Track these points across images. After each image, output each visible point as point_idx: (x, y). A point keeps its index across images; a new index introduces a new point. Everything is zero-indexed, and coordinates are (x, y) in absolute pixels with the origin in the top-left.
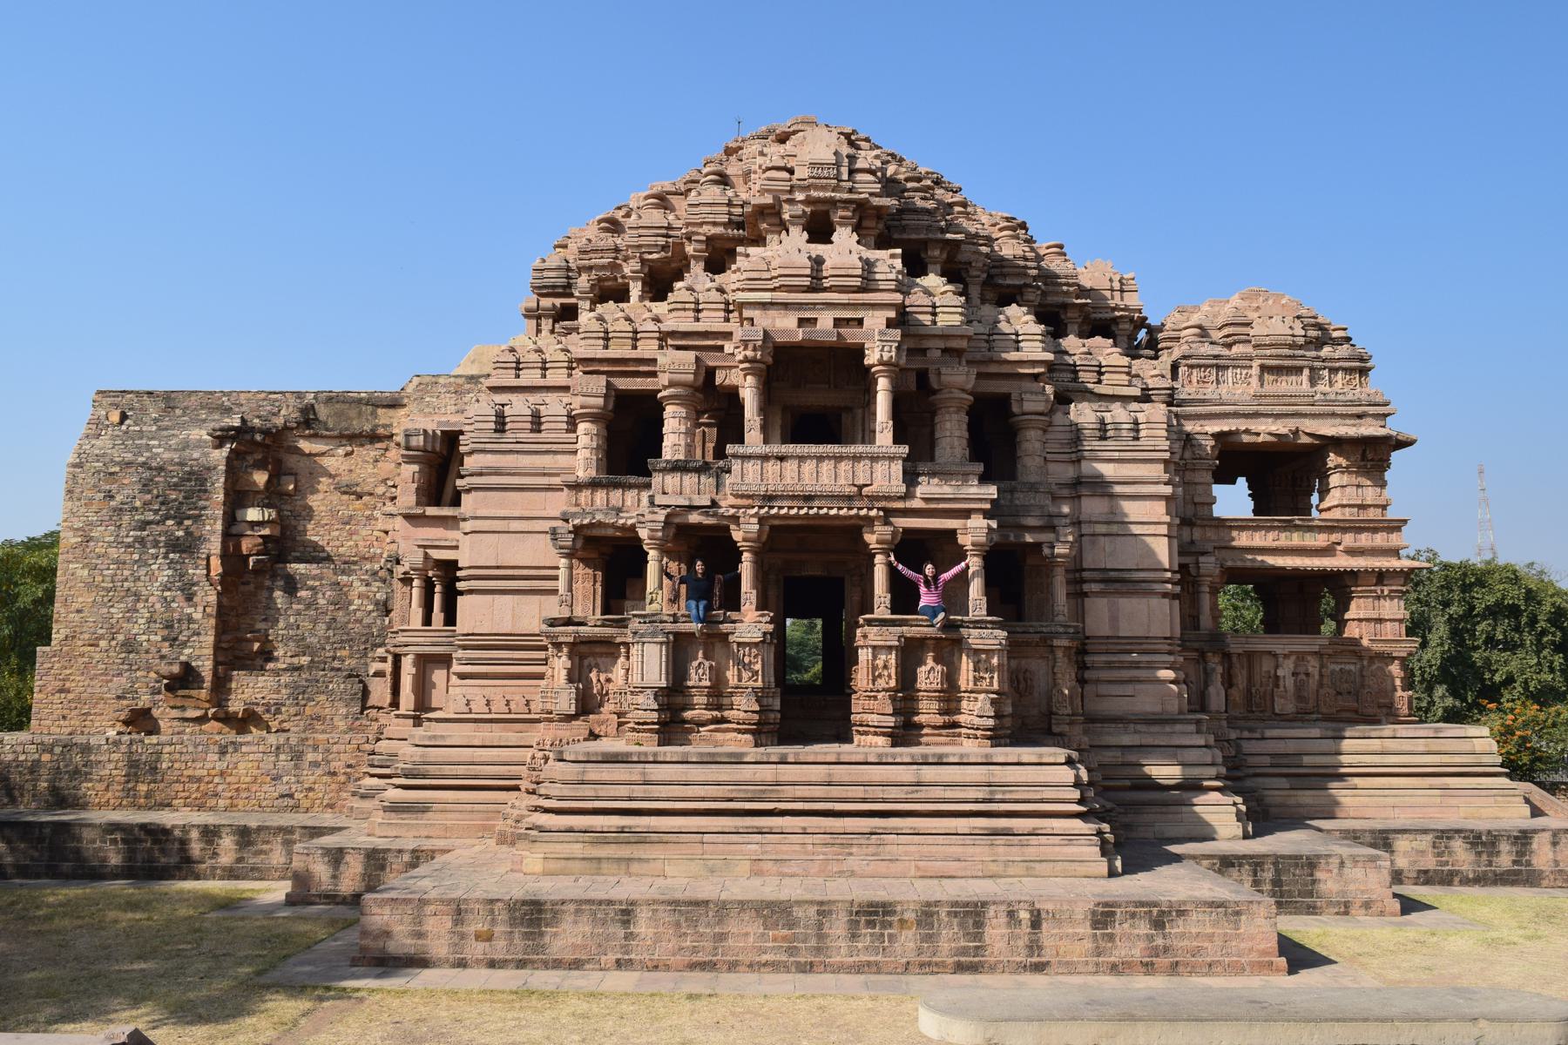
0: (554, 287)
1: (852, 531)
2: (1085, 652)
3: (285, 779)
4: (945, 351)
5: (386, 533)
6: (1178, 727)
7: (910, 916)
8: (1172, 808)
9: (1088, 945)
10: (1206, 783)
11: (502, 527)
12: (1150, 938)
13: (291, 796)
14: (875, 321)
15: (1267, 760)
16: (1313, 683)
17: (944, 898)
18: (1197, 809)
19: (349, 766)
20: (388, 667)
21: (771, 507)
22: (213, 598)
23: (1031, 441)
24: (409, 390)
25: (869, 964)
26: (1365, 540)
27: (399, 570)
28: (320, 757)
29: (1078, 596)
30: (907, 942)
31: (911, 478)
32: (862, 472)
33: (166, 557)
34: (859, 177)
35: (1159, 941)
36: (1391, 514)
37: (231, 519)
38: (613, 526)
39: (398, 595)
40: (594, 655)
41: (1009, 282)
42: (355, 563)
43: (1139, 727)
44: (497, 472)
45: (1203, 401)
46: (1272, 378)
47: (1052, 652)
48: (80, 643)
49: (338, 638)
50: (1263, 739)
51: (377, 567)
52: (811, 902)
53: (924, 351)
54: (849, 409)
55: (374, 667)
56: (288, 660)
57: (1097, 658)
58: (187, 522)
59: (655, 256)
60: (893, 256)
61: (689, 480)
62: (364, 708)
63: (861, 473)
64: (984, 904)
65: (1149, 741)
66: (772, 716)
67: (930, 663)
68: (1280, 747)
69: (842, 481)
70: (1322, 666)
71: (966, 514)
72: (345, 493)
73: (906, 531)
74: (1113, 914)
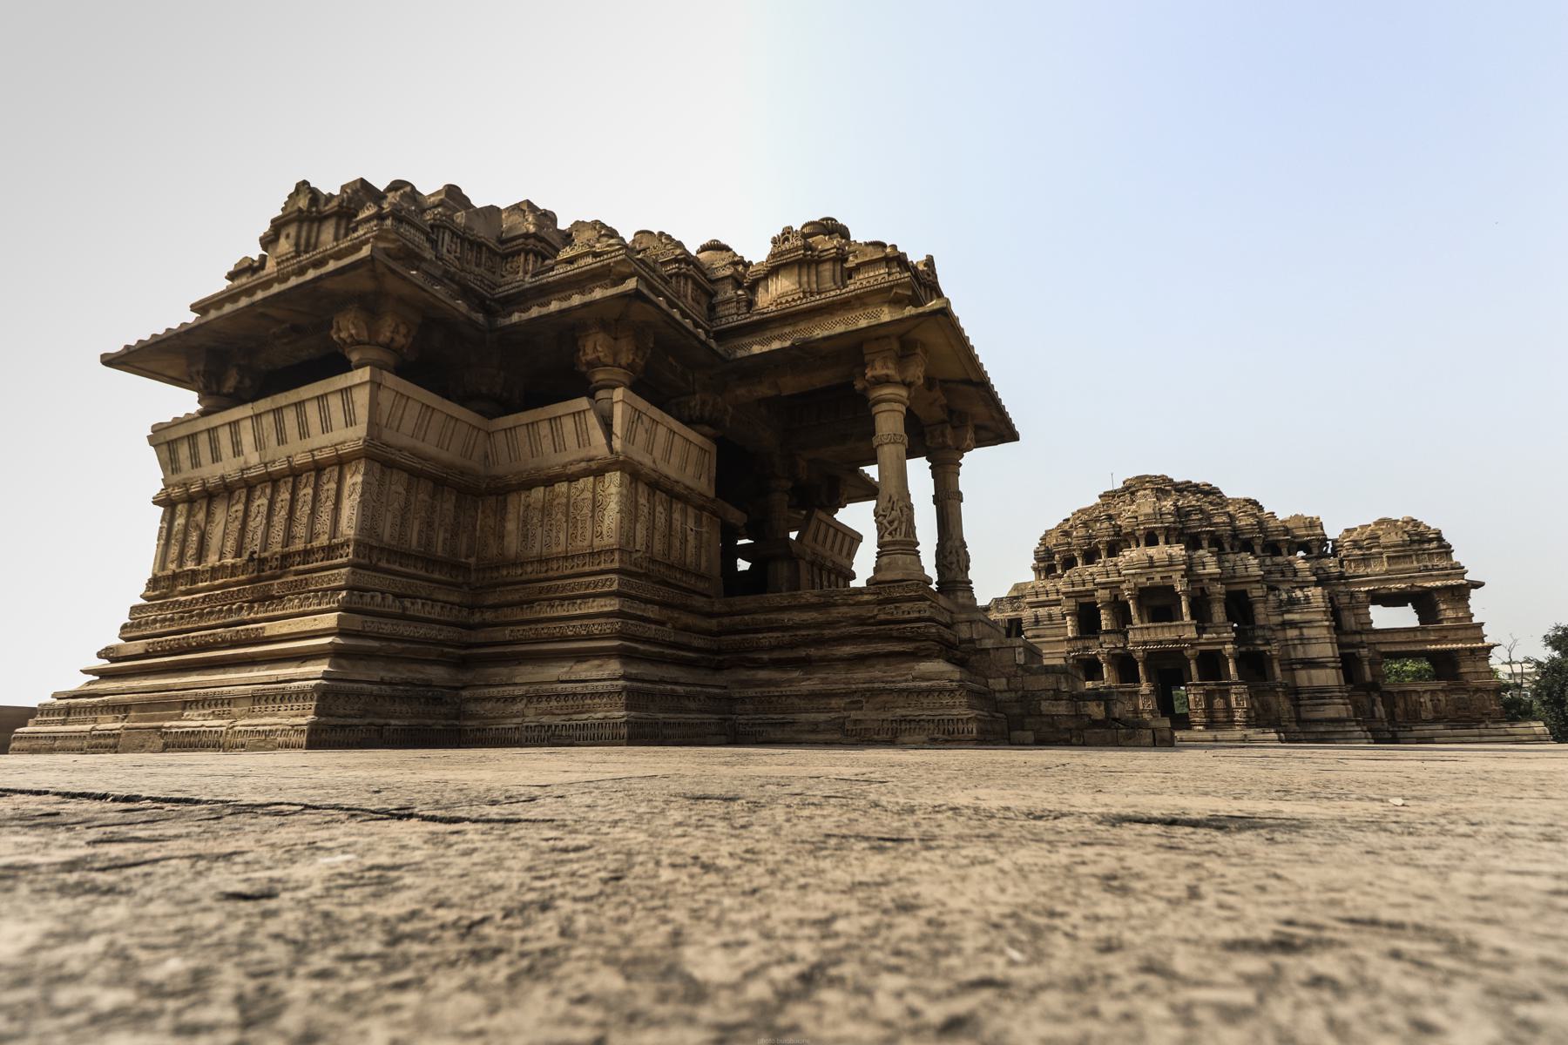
14: (1177, 576)
16: (1443, 704)
71: (1225, 643)
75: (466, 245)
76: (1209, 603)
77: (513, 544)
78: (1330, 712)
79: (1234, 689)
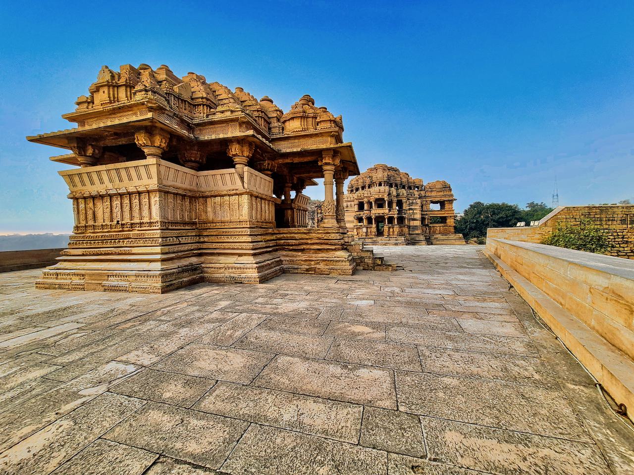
1: (384, 216)
14: (386, 196)
26: (449, 212)
31: (390, 211)
73: (389, 217)
75: (180, 101)
77: (211, 216)
78: (417, 232)
79: (395, 226)
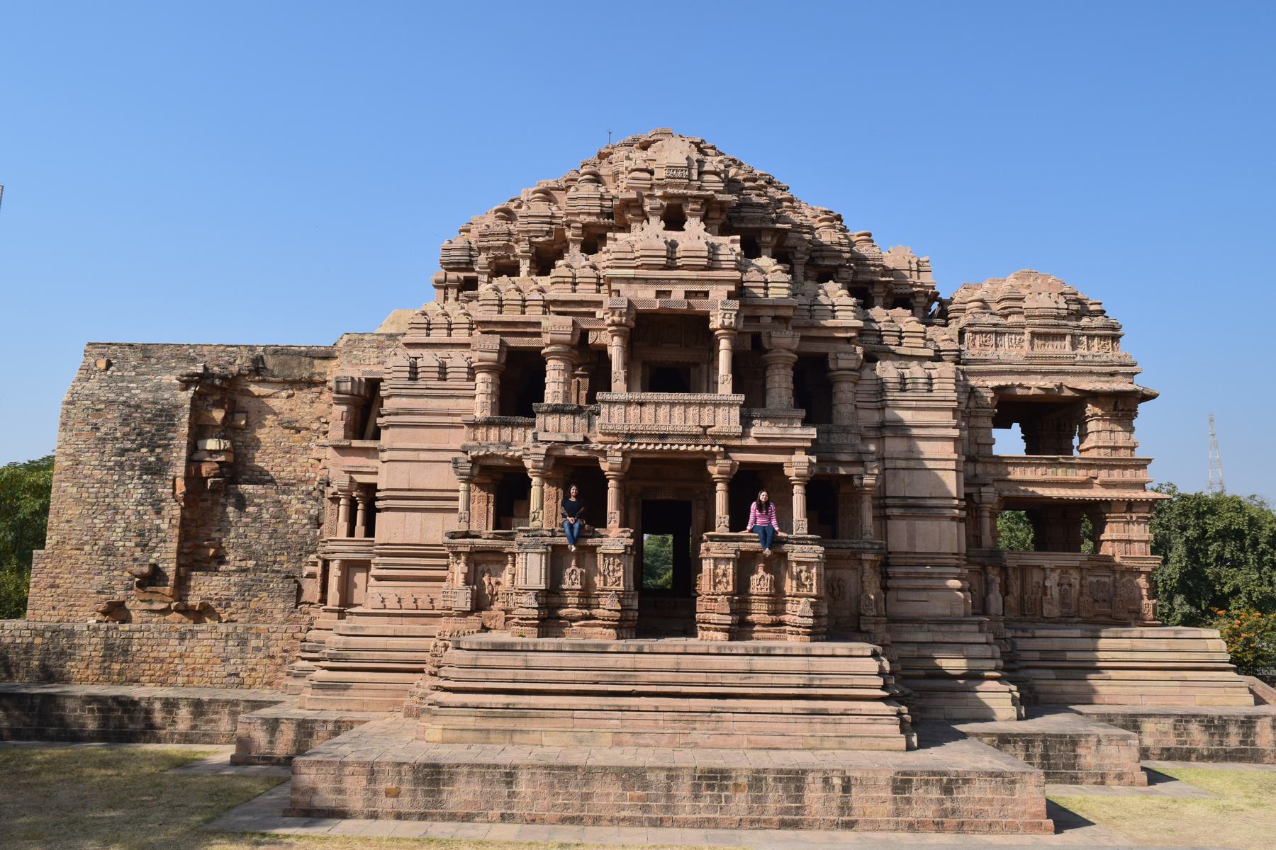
0: (459, 263)
1: (699, 463)
2: (888, 565)
3: (232, 661)
4: (775, 318)
5: (319, 460)
6: (964, 627)
7: (743, 781)
8: (960, 694)
9: (889, 807)
10: (986, 674)
11: (413, 457)
12: (941, 802)
13: (237, 675)
14: (719, 293)
15: (1037, 655)
17: (771, 766)
18: (979, 695)
19: (285, 651)
20: (318, 570)
21: (633, 444)
22: (177, 512)
23: (845, 392)
24: (340, 345)
25: (709, 820)
26: (1116, 475)
27: (329, 491)
28: (261, 644)
29: (882, 518)
30: (740, 802)
31: (746, 421)
32: (707, 416)
33: (140, 478)
34: (707, 177)
35: (948, 805)
36: (1139, 454)
37: (193, 448)
38: (503, 457)
39: (328, 512)
40: (487, 562)
41: (827, 263)
42: (293, 485)
43: (932, 627)
44: (410, 412)
45: (985, 361)
46: (1040, 342)
47: (861, 564)
48: (68, 547)
49: (278, 545)
50: (1034, 637)
51: (311, 488)
52: (662, 768)
53: (758, 318)
54: (696, 365)
55: (307, 570)
56: (237, 563)
57: (897, 570)
58: (158, 450)
59: (541, 239)
60: (733, 241)
61: (566, 421)
62: (298, 603)
63: (706, 417)
64: (804, 772)
65: (939, 638)
66: (631, 614)
67: (761, 572)
68: (1047, 644)
69: (690, 423)
70: (1082, 578)
71: (791, 450)
72: (286, 428)
73: (742, 464)
74: (910, 781)
76: (765, 367)
